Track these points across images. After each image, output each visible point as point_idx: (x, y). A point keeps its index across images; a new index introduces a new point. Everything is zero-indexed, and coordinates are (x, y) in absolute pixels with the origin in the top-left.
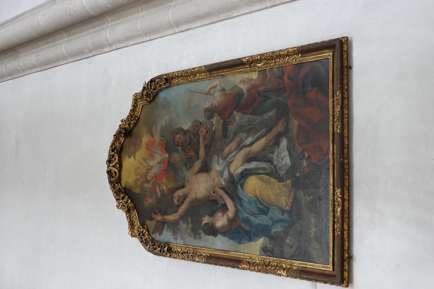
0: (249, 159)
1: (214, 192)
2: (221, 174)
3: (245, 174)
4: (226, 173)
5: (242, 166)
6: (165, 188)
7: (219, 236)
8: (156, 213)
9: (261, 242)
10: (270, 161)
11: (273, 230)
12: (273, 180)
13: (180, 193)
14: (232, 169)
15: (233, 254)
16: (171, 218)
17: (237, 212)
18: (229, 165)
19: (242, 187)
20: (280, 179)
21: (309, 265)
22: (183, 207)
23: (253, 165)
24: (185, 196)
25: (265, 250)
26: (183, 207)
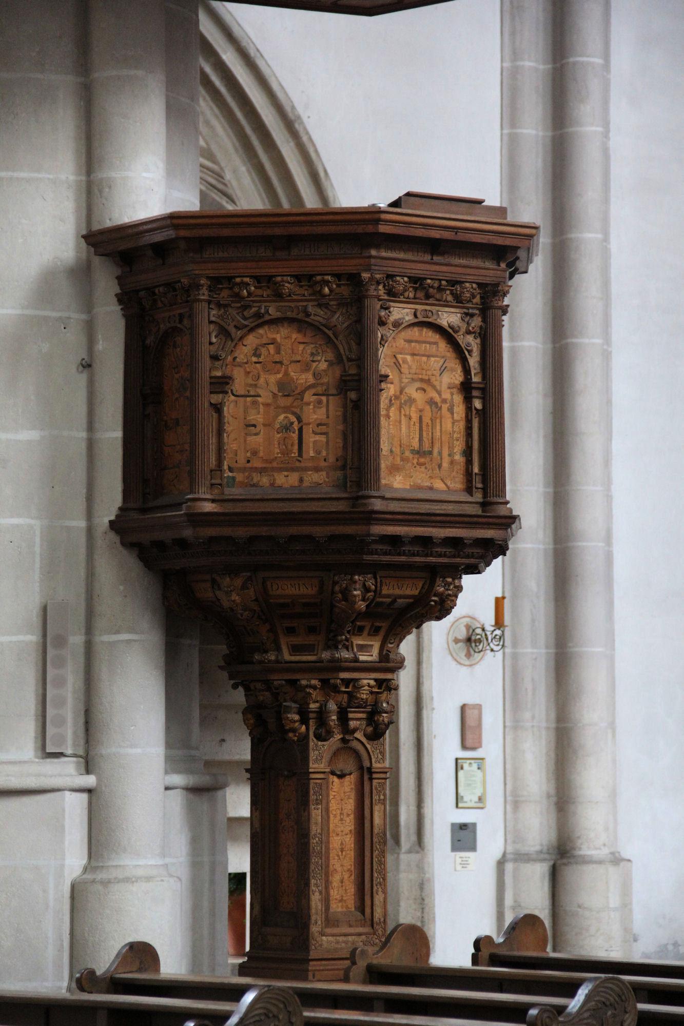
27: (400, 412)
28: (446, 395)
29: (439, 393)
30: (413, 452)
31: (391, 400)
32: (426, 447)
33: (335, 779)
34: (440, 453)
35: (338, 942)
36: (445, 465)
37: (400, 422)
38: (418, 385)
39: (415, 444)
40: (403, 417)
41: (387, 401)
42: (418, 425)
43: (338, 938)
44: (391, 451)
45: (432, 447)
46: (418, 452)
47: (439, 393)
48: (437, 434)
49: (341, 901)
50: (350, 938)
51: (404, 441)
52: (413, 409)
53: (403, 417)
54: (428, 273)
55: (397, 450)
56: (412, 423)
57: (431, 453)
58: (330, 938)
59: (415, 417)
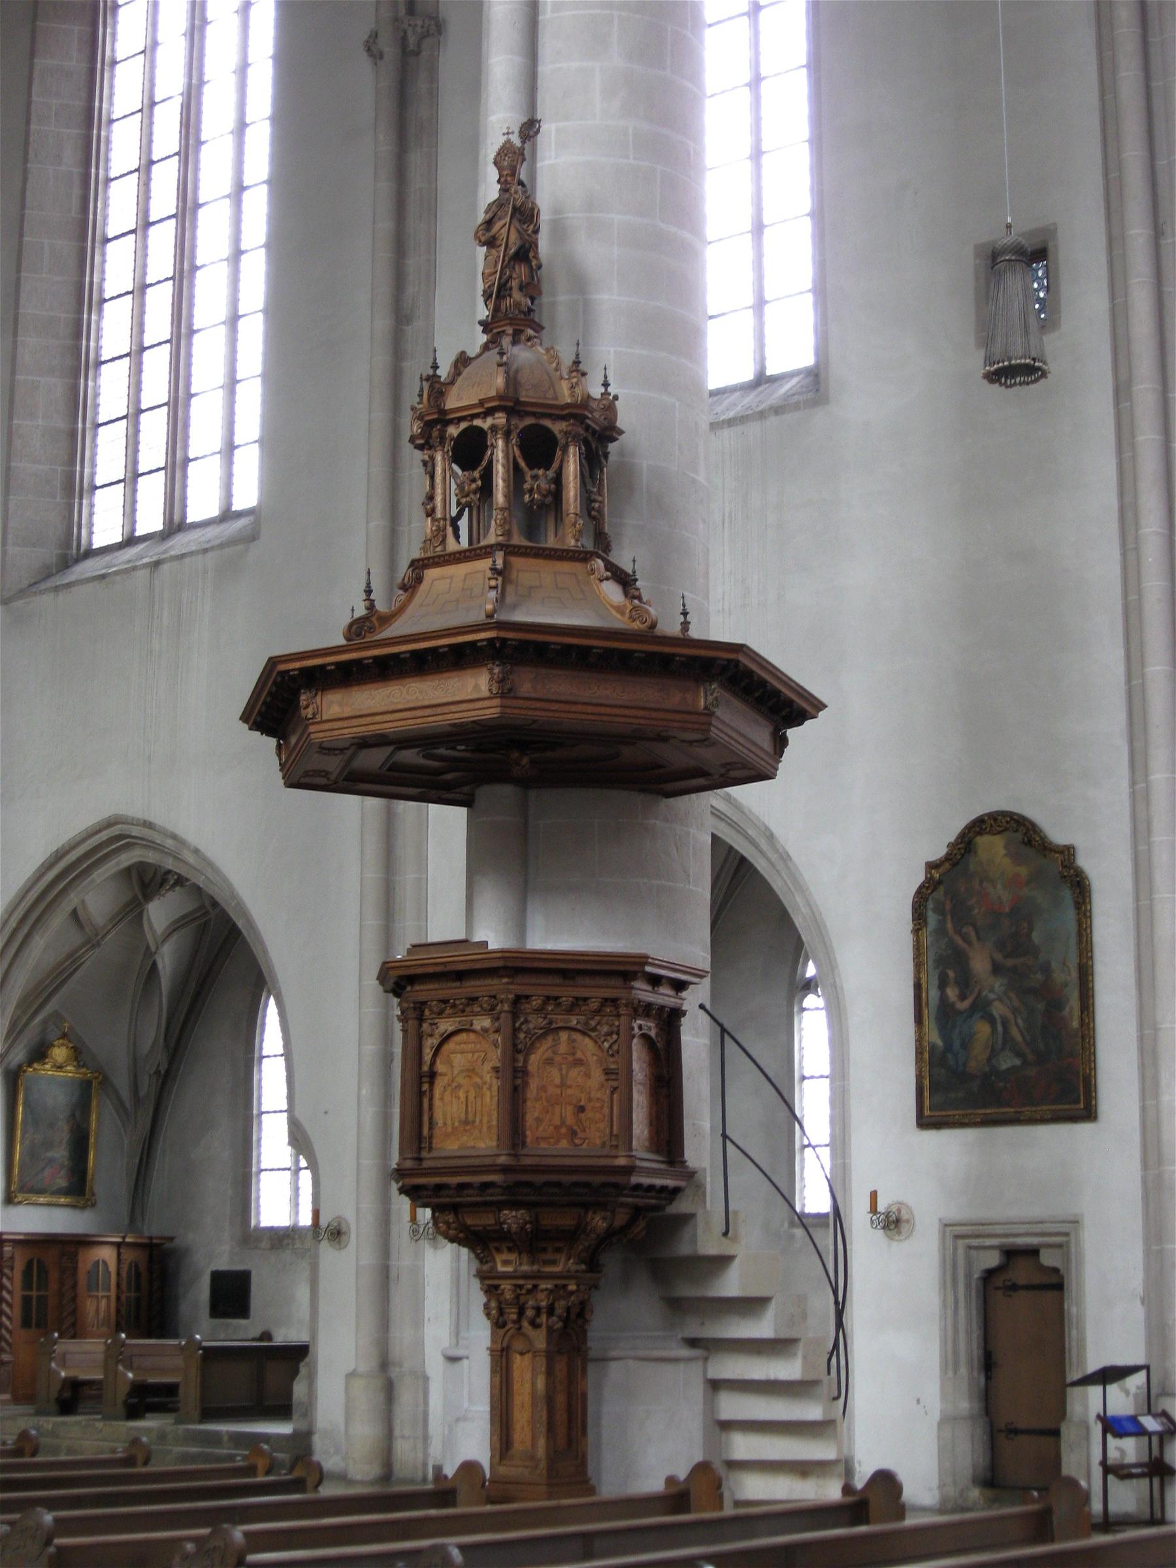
0: (1005, 1024)
1: (976, 982)
2: (992, 990)
3: (992, 1021)
4: (992, 996)
5: (1001, 1017)
6: (976, 911)
7: (939, 993)
8: (951, 901)
9: (940, 1043)
10: (1003, 1049)
11: (949, 1056)
12: (988, 1052)
13: (973, 934)
14: (997, 1004)
15: (925, 1012)
16: (949, 925)
17: (960, 1013)
18: (1000, 999)
19: (982, 1017)
20: (989, 1060)
21: (927, 1094)
22: (959, 941)
23: (1000, 1028)
24: (970, 943)
25: (933, 1048)
26: (959, 941)
28: (487, 1078)
29: (481, 1078)
32: (471, 1117)
33: (518, 1356)
34: (481, 1121)
36: (485, 1129)
37: (451, 1102)
38: (465, 1074)
39: (463, 1116)
41: (442, 1089)
45: (475, 1117)
47: (481, 1078)
48: (479, 1108)
52: (461, 1090)
53: (454, 1099)
57: (474, 1122)
59: (463, 1099)
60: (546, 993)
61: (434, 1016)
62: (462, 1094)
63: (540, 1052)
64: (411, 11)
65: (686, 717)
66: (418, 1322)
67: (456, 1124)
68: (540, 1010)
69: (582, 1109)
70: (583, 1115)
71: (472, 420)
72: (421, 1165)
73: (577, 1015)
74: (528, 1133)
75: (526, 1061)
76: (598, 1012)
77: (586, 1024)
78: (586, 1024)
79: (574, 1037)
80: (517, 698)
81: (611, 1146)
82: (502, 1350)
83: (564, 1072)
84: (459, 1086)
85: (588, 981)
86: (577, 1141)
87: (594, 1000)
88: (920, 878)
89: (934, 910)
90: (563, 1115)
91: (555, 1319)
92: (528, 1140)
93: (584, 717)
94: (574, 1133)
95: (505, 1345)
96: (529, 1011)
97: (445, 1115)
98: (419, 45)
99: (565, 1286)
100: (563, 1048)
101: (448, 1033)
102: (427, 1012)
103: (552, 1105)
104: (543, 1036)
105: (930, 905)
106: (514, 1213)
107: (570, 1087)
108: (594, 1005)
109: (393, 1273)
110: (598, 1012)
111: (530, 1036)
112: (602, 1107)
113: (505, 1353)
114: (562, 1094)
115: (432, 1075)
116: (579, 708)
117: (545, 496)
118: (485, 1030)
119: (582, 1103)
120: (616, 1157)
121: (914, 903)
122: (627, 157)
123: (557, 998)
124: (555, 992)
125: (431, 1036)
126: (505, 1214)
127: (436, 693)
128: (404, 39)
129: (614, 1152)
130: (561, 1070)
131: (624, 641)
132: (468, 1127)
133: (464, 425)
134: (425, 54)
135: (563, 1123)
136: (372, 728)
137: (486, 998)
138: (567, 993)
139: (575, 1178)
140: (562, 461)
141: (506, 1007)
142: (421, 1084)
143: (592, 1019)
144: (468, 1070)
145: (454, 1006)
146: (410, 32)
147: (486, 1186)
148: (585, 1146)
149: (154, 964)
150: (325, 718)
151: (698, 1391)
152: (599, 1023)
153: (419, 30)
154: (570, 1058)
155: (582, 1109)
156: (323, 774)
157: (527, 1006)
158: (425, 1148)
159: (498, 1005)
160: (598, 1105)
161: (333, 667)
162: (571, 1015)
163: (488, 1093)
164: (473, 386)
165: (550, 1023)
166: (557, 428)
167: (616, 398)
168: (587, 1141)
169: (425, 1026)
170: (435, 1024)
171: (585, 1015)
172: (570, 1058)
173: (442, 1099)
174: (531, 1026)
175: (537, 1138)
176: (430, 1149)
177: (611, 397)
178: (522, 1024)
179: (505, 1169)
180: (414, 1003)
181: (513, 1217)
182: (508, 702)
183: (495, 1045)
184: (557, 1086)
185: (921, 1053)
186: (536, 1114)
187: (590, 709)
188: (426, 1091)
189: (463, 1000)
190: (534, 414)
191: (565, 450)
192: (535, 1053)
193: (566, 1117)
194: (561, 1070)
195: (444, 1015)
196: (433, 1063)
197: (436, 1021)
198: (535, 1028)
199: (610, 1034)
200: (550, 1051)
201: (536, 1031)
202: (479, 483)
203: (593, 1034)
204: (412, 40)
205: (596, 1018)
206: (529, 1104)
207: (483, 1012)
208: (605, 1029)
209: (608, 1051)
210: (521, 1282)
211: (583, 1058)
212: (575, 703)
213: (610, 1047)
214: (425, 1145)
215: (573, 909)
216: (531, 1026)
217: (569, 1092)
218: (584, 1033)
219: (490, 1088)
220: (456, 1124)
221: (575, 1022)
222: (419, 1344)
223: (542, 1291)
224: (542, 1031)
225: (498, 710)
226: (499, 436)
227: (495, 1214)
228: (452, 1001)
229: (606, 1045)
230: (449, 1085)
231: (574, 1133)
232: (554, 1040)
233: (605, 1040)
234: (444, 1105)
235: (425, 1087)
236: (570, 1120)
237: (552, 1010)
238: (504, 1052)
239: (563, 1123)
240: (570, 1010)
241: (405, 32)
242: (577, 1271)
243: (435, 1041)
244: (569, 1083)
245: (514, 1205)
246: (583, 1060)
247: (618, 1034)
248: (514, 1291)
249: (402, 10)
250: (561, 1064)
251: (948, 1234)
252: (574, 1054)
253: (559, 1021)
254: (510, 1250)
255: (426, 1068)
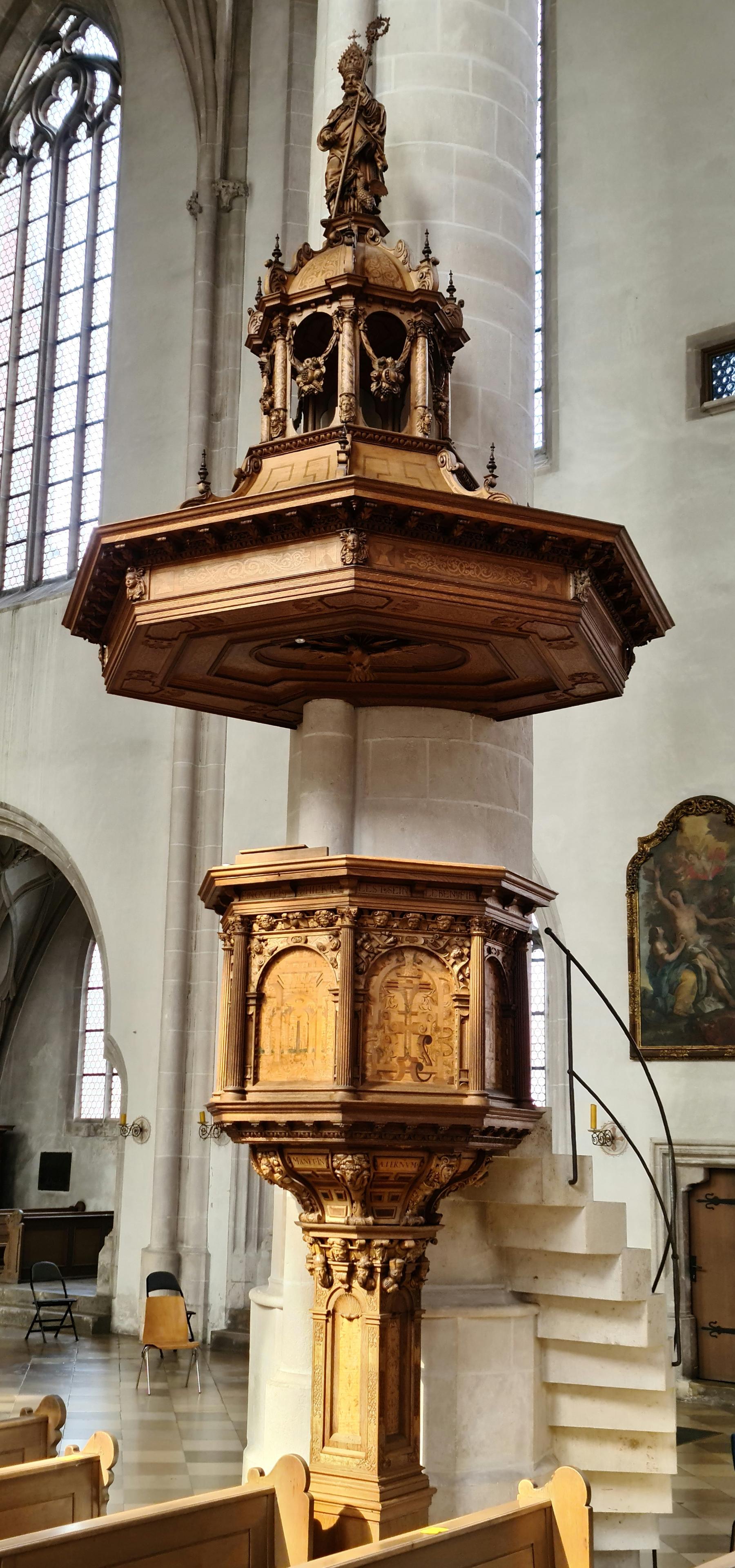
0: (709, 972)
1: (682, 938)
2: (697, 945)
3: (696, 970)
4: (697, 950)
5: (704, 966)
6: (683, 878)
7: (650, 946)
8: (660, 870)
9: (651, 988)
10: (707, 995)
11: (659, 999)
12: (694, 997)
13: (680, 898)
14: (701, 956)
15: (638, 962)
16: (659, 890)
17: (668, 963)
18: (704, 953)
19: (687, 968)
20: (695, 1003)
22: (667, 902)
23: (704, 977)
24: (676, 905)
25: (644, 991)
26: (667, 902)
27: (281, 1020)
30: (290, 1051)
31: (273, 1011)
35: (334, 1461)
37: (281, 1028)
40: (283, 1024)
41: (271, 1013)
42: (296, 1029)
43: (335, 1457)
44: (272, 1052)
46: (295, 1051)
48: (312, 1035)
49: (348, 1425)
50: (345, 1459)
51: (285, 1043)
52: (292, 1016)
53: (283, 1024)
54: (281, 908)
55: (277, 1051)
56: (291, 1028)
57: (306, 1051)
58: (328, 1456)
60: (393, 907)
61: (263, 931)
62: (293, 1021)
63: (382, 974)
64: (225, 176)
65: (555, 606)
66: (203, 1207)
67: (286, 1053)
68: (385, 927)
69: (428, 1040)
70: (428, 1046)
71: (316, 307)
72: (245, 1099)
73: (424, 933)
74: (369, 1065)
75: (368, 983)
76: (448, 931)
77: (435, 944)
78: (435, 944)
79: (421, 958)
80: (374, 570)
81: (461, 1082)
82: (328, 1314)
83: (409, 997)
84: (290, 1010)
85: (436, 895)
86: (423, 1077)
87: (443, 917)
88: (634, 850)
89: (645, 878)
90: (407, 1047)
91: (390, 1280)
92: (369, 1073)
93: (445, 597)
94: (419, 1066)
95: (330, 1308)
96: (371, 927)
97: (273, 1042)
98: (230, 203)
99: (401, 1242)
100: (407, 971)
101: (278, 950)
102: (256, 927)
103: (395, 1034)
104: (388, 956)
105: (642, 873)
106: (349, 1158)
107: (416, 1014)
108: (443, 923)
109: (184, 1164)
110: (448, 931)
111: (372, 955)
112: (450, 1038)
113: (330, 1319)
114: (406, 1022)
115: (260, 998)
116: (440, 587)
117: (392, 384)
118: (323, 949)
119: (428, 1033)
120: (466, 1096)
121: (628, 870)
122: (467, 90)
123: (403, 914)
124: (402, 906)
125: (260, 953)
126: (338, 1159)
127: (280, 567)
128: (219, 198)
129: (463, 1091)
130: (405, 995)
131: (496, 512)
132: (298, 1057)
133: (307, 313)
134: (235, 210)
135: (407, 1054)
136: (206, 607)
137: (324, 912)
138: (414, 909)
139: (421, 1119)
140: (410, 353)
141: (347, 922)
142: (246, 1007)
143: (441, 938)
144: (301, 992)
145: (287, 920)
146: (223, 192)
147: (319, 1126)
148: (430, 1082)
149: (8, 915)
150: (152, 598)
151: (529, 1351)
152: (448, 944)
153: (231, 190)
154: (416, 982)
155: (428, 1040)
156: (148, 676)
157: (371, 921)
158: (250, 1079)
159: (337, 920)
160: (446, 1035)
161: (164, 538)
162: (417, 933)
163: (324, 1018)
164: (318, 273)
165: (395, 942)
166: (406, 318)
167: (462, 304)
168: (433, 1076)
169: (255, 944)
170: (264, 940)
171: (433, 934)
172: (416, 982)
173: (270, 1024)
174: (374, 944)
175: (379, 1071)
176: (256, 1080)
177: (457, 303)
178: (364, 941)
179: (344, 1108)
180: (242, 916)
181: (349, 1161)
182: (363, 575)
183: (332, 964)
184: (401, 1013)
185: (634, 996)
186: (378, 1044)
187: (452, 589)
188: (252, 1014)
189: (297, 914)
190: (382, 301)
191: (414, 342)
192: (377, 975)
193: (410, 1047)
194: (405, 995)
195: (275, 931)
196: (261, 983)
197: (265, 937)
198: (378, 947)
199: (460, 957)
200: (394, 973)
201: (380, 950)
202: (324, 369)
203: (442, 957)
204: (225, 198)
205: (445, 937)
206: (370, 1032)
207: (320, 928)
208: (456, 952)
209: (458, 976)
210: (354, 1236)
211: (430, 981)
212: (438, 581)
213: (461, 971)
214: (250, 1075)
215: (403, 830)
216: (374, 944)
217: (414, 1019)
218: (431, 954)
219: (325, 1014)
220: (286, 1053)
221: (423, 942)
222: (202, 1226)
223: (376, 1247)
224: (386, 950)
225: (352, 582)
226: (346, 319)
227: (327, 1158)
228: (285, 915)
229: (456, 968)
230: (278, 1009)
231: (419, 1066)
232: (398, 961)
233: (455, 963)
234: (271, 1031)
235: (252, 1010)
236: (415, 1052)
237: (397, 927)
238: (344, 972)
239: (407, 1054)
240: (417, 929)
241: (220, 192)
242: (416, 1225)
243: (265, 959)
244: (414, 1010)
245: (348, 1149)
246: (429, 985)
247: (469, 956)
248: (344, 1247)
249: (218, 176)
250: (406, 988)
251: (658, 1152)
252: (419, 977)
253: (404, 939)
254: (340, 1197)
255: (253, 989)
